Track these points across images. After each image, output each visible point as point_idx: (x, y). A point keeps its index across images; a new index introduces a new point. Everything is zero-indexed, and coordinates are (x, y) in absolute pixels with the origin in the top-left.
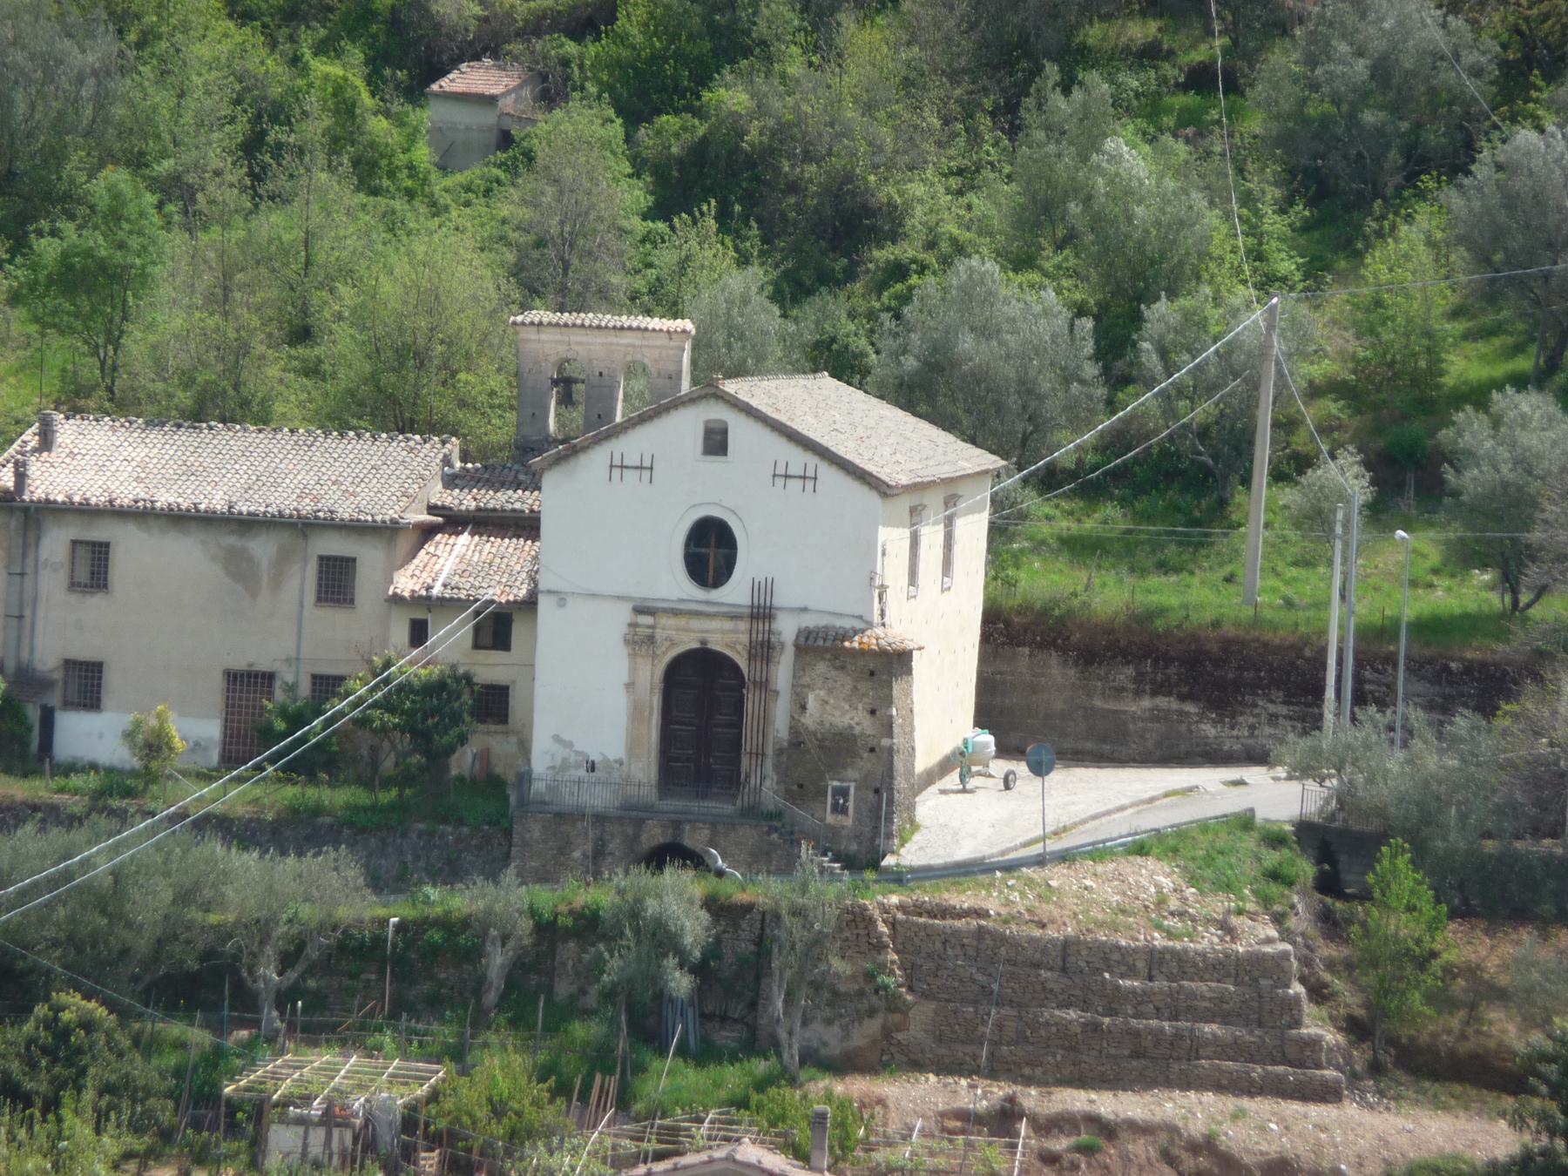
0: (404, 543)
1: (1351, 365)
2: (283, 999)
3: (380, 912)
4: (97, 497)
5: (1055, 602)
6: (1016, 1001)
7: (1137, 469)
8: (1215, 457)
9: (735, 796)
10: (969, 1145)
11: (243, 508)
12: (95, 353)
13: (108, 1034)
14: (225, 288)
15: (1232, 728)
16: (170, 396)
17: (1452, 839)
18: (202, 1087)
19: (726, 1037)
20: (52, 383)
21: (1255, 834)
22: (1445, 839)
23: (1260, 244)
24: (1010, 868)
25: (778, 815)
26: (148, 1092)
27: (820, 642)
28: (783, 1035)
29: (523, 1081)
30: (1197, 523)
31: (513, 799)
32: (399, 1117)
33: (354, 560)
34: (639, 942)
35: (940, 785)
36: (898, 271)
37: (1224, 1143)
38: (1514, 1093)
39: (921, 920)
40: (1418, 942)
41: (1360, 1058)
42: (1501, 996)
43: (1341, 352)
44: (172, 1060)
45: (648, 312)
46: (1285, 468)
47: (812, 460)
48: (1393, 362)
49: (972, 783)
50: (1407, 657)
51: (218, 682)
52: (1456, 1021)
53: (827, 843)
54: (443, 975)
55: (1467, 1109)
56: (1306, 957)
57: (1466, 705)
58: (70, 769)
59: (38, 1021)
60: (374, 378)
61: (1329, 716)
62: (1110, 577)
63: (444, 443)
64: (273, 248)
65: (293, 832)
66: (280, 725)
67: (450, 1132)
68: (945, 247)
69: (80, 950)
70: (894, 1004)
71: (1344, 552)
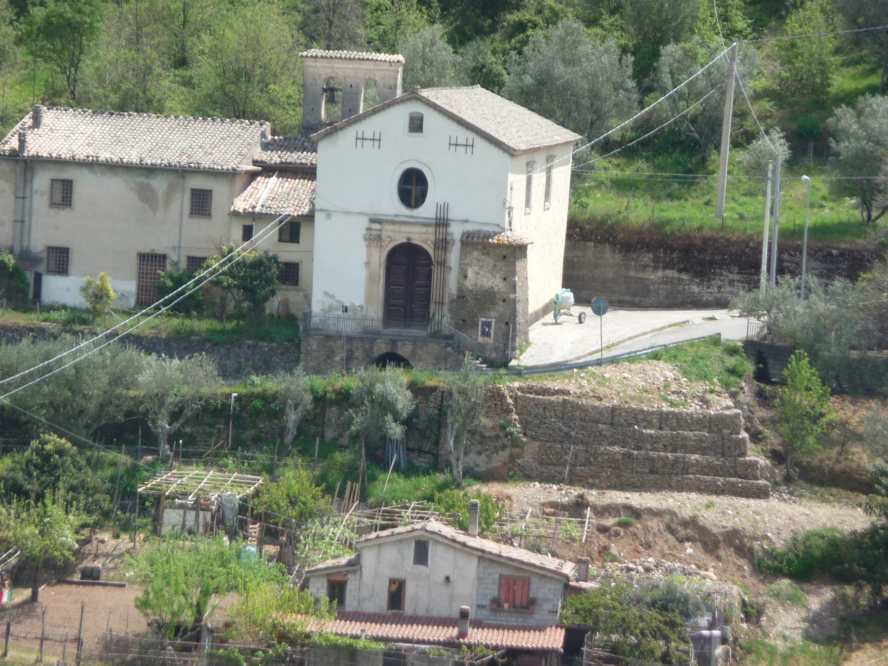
0: (239, 182)
1: (778, 81)
2: (172, 439)
3: (227, 390)
4: (65, 154)
5: (609, 216)
6: (588, 443)
7: (656, 141)
8: (700, 134)
9: (426, 326)
10: (558, 522)
11: (148, 161)
12: (64, 72)
13: (73, 457)
14: (137, 36)
15: (709, 288)
16: (106, 97)
17: (832, 351)
18: (125, 488)
19: (421, 461)
20: (40, 89)
21: (721, 348)
22: (829, 351)
23: (727, 12)
24: (582, 367)
25: (451, 337)
26: (96, 490)
27: (475, 239)
28: (453, 461)
29: (307, 484)
30: (689, 171)
31: (301, 328)
32: (237, 505)
33: (211, 191)
34: (373, 407)
35: (542, 320)
36: (521, 27)
37: (701, 521)
38: (866, 493)
39: (532, 396)
40: (813, 408)
41: (779, 473)
42: (859, 438)
43: (772, 73)
44: (109, 472)
45: (378, 51)
46: (740, 140)
47: (471, 135)
48: (802, 79)
49: (561, 319)
50: (808, 247)
51: (134, 261)
52: (834, 453)
53: (478, 352)
54: (262, 426)
55: (839, 502)
56: (749, 417)
57: (840, 275)
58: (51, 308)
59: (33, 450)
60: (222, 87)
61: (763, 281)
62: (640, 203)
63: (261, 125)
64: (165, 13)
65: (177, 345)
66: (169, 283)
67: (266, 514)
68: (547, 13)
69: (56, 409)
70: (515, 443)
71: (773, 187)
